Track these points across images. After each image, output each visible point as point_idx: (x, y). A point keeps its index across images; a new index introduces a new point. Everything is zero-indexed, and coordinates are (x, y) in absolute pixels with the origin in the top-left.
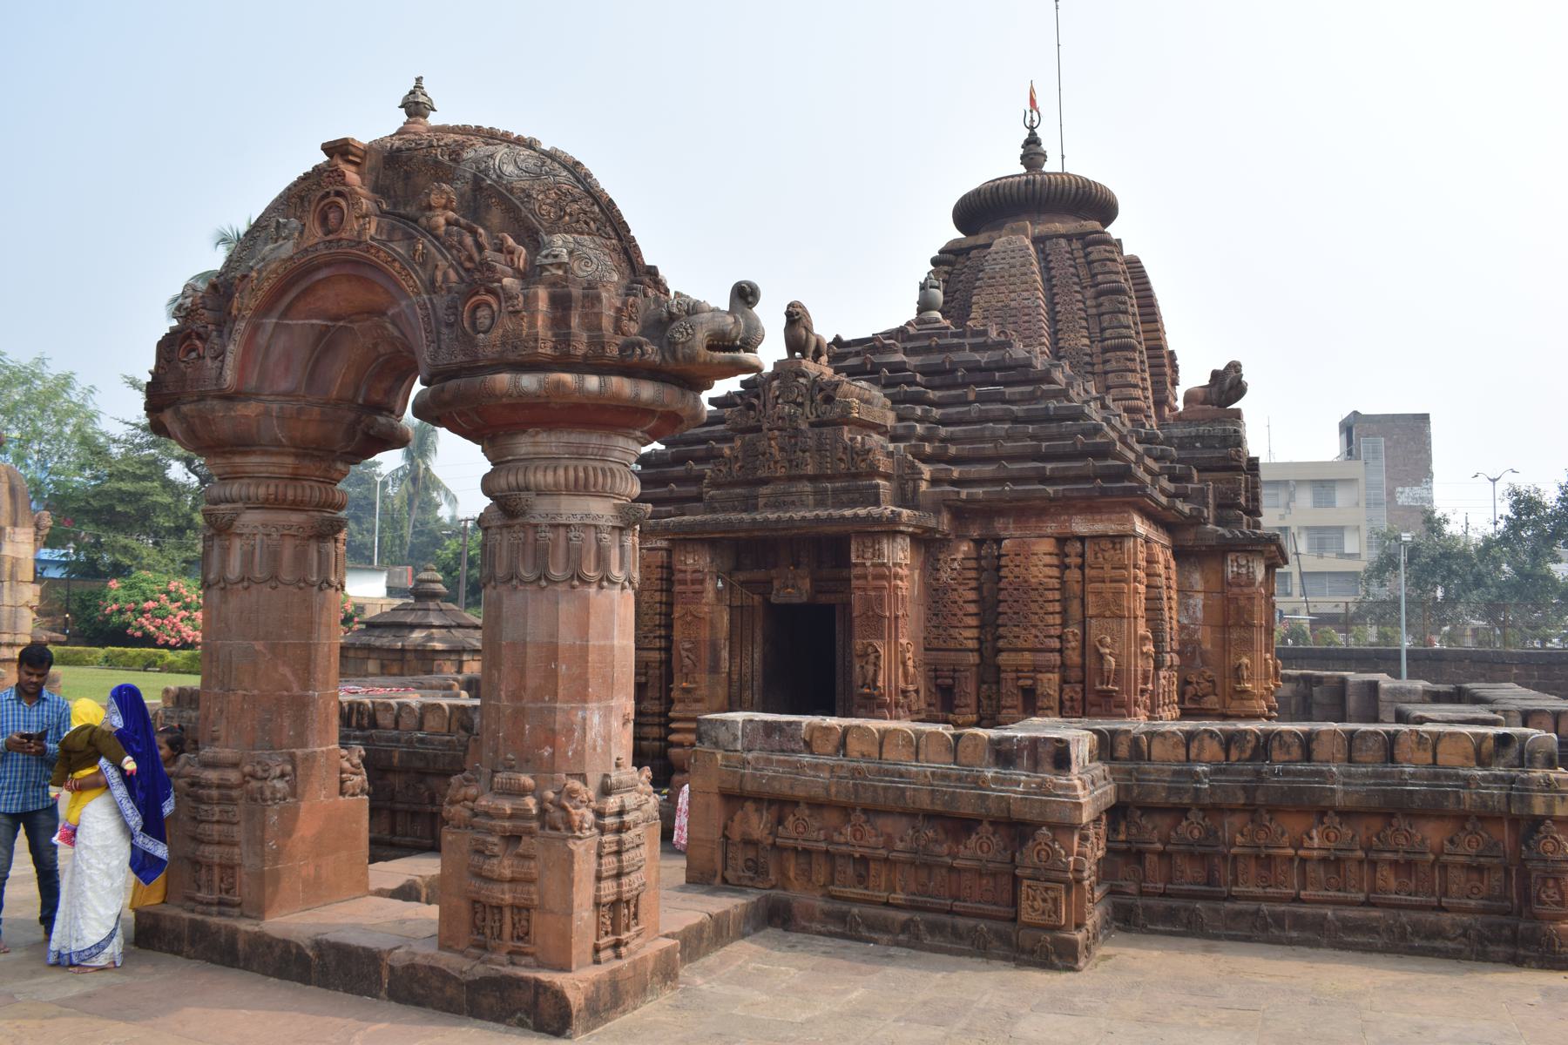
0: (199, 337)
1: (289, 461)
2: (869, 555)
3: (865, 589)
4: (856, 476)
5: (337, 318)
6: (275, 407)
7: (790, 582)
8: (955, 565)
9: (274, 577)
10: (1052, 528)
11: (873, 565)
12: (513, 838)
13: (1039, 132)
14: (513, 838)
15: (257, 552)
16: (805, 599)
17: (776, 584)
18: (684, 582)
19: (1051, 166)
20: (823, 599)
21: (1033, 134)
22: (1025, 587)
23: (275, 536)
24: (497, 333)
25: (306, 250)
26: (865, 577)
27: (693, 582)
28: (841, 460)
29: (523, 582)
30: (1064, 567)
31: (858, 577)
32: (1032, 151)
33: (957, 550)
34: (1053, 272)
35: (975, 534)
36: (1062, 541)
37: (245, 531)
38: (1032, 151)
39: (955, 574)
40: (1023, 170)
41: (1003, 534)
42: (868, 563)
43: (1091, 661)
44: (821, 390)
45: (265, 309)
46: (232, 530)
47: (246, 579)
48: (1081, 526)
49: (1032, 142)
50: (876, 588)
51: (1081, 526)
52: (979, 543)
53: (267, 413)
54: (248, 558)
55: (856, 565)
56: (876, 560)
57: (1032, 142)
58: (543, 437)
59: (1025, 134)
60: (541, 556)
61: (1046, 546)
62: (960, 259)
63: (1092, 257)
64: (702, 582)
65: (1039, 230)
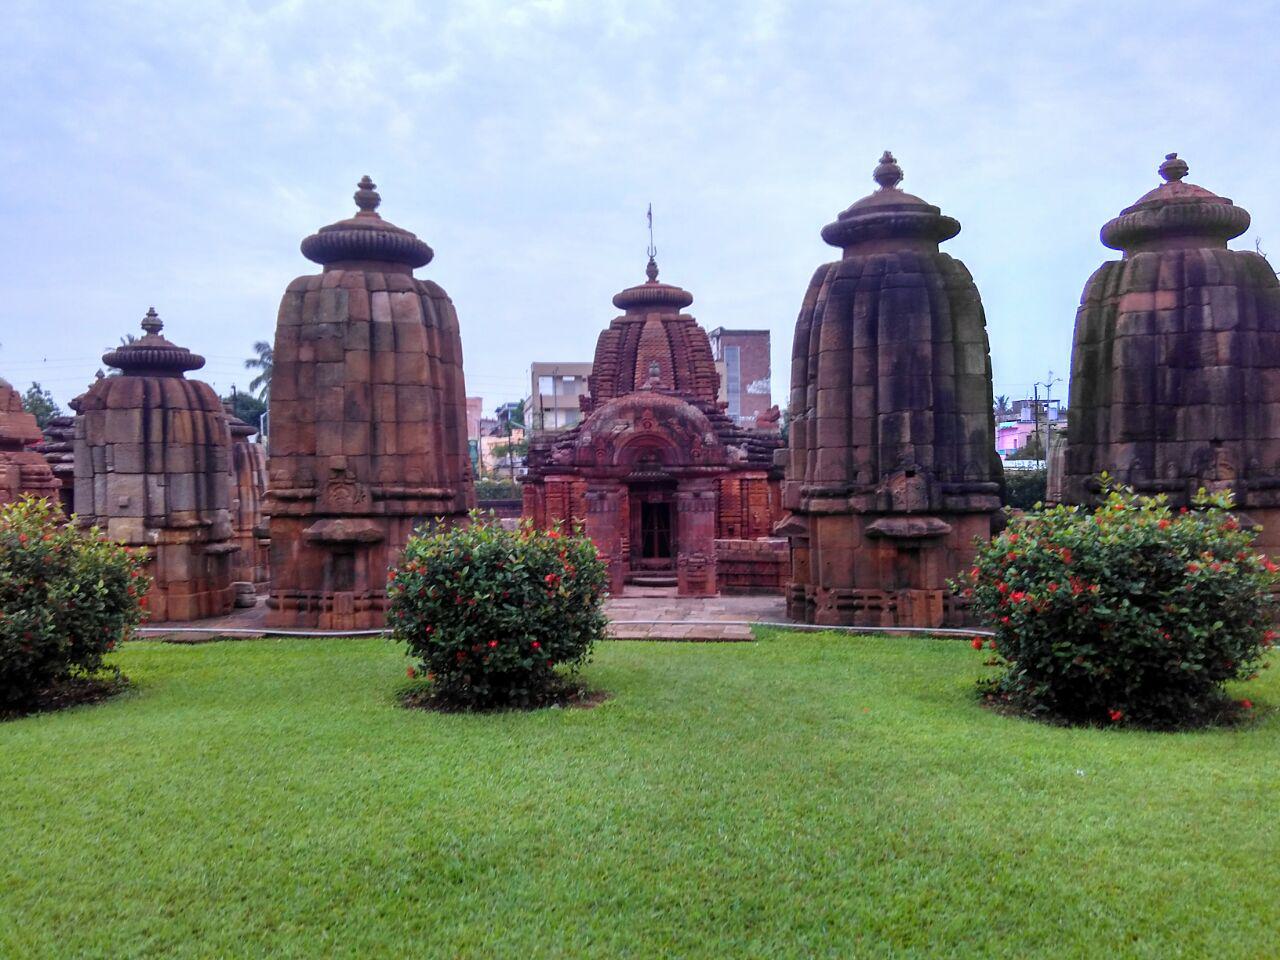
10: (739, 476)
12: (699, 567)
13: (656, 260)
14: (699, 567)
19: (663, 279)
21: (652, 260)
22: (730, 496)
24: (701, 458)
30: (742, 489)
32: (652, 270)
36: (742, 480)
38: (652, 270)
40: (647, 279)
43: (751, 520)
47: (609, 511)
48: (748, 476)
51: (748, 476)
54: (609, 507)
60: (703, 507)
61: (737, 483)
65: (665, 316)
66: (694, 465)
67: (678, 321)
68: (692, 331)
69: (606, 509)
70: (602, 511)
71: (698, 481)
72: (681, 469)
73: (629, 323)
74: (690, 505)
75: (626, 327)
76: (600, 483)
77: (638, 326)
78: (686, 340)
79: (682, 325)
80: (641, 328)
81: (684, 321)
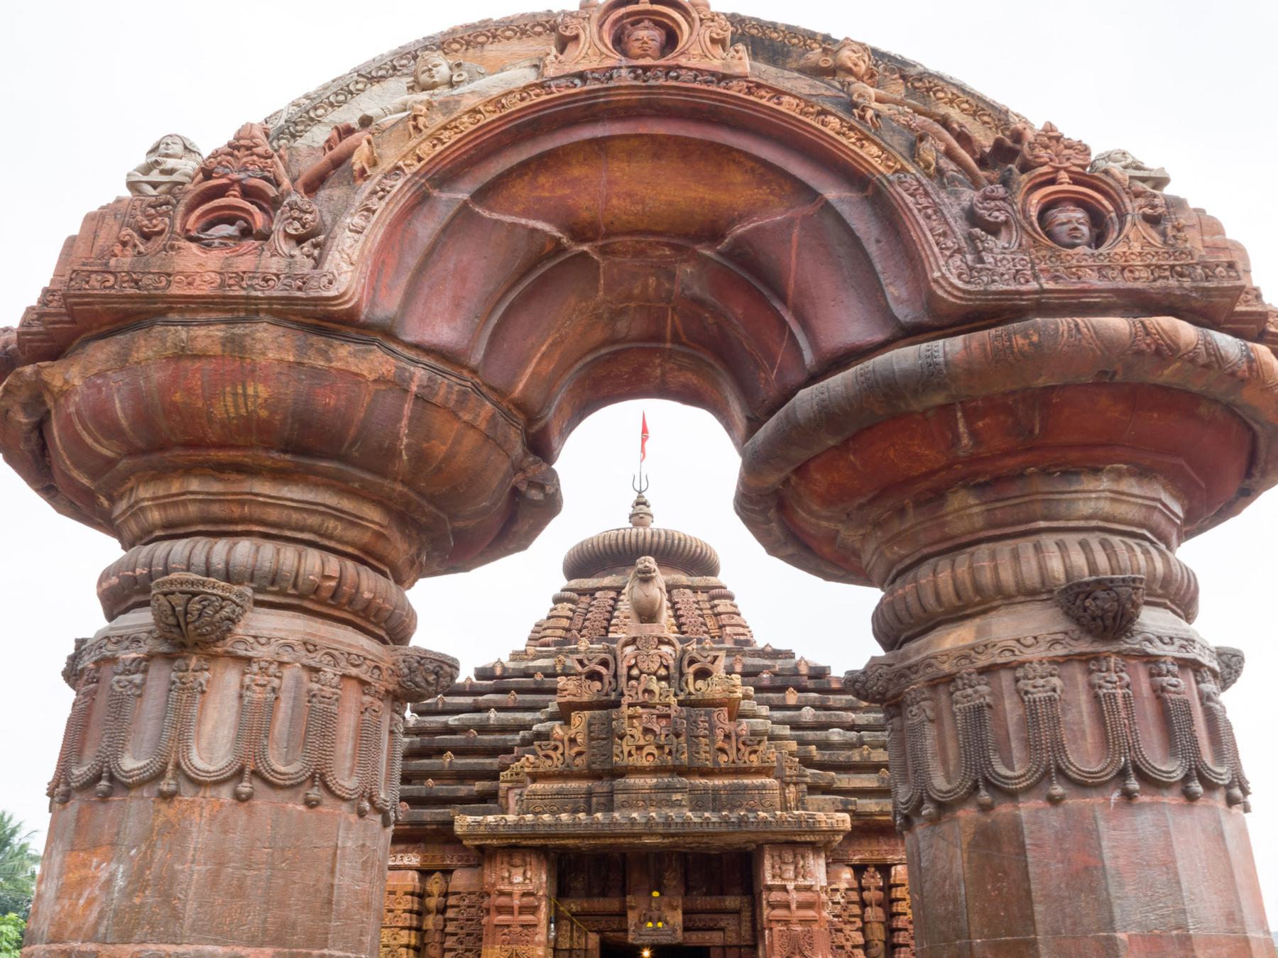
0: (250, 193)
1: (373, 514)
2: (791, 874)
3: (787, 922)
4: (746, 772)
5: (579, 233)
6: (420, 374)
7: (656, 914)
8: (838, 897)
9: (319, 778)
11: (797, 889)
15: (284, 707)
16: (679, 937)
17: (632, 918)
18: (508, 910)
20: (696, 939)
23: (329, 673)
25: (581, 76)
26: (787, 906)
27: (523, 910)
28: (722, 750)
29: (1152, 783)
31: (773, 906)
33: (839, 878)
34: (683, 620)
35: (856, 859)
37: (259, 652)
39: (838, 910)
41: (890, 858)
42: (791, 886)
44: (692, 661)
45: (444, 174)
46: (228, 645)
47: (248, 774)
49: (640, 502)
50: (802, 921)
52: (859, 870)
53: (398, 385)
54: (254, 724)
55: (770, 889)
56: (801, 882)
57: (640, 502)
58: (1130, 486)
59: (634, 496)
62: (583, 598)
63: (720, 609)
64: (534, 910)
66: (1079, 304)
67: (695, 589)
68: (723, 606)
69: (212, 749)
70: (170, 779)
71: (1096, 495)
72: (949, 348)
73: (591, 592)
74: (1041, 720)
75: (586, 599)
76: (219, 528)
77: (613, 594)
78: (710, 622)
79: (704, 597)
80: (616, 600)
81: (706, 589)
